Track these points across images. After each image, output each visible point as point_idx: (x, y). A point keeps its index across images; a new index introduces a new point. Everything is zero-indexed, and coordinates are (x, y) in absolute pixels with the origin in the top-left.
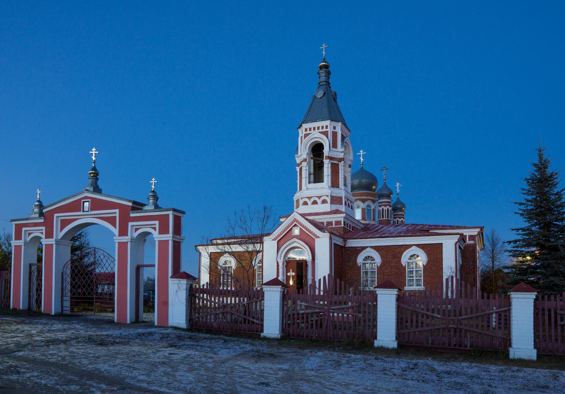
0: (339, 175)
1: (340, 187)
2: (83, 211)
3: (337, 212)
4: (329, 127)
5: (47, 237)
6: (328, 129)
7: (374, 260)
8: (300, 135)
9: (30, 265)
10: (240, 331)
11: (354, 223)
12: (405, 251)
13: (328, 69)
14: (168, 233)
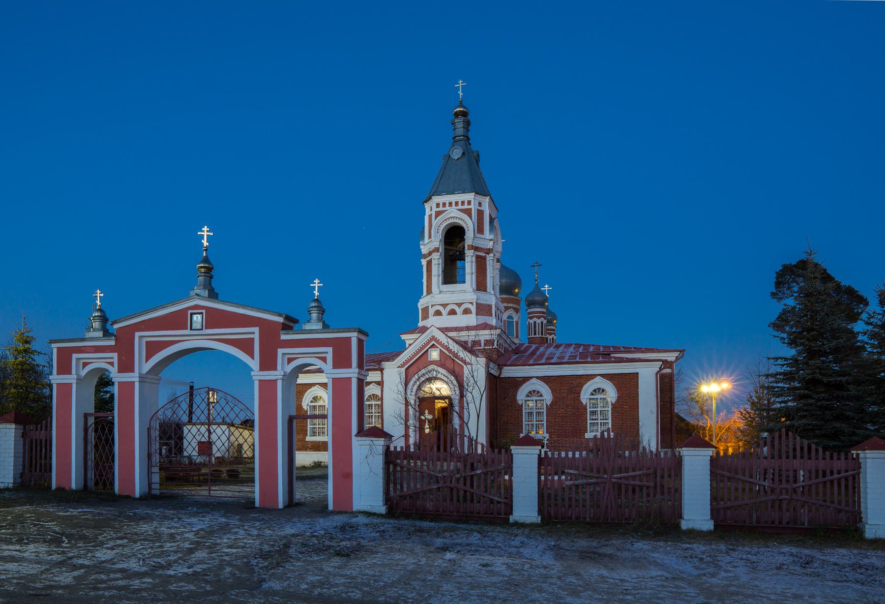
0: (486, 274)
1: (488, 290)
2: (191, 329)
3: (485, 326)
4: (472, 203)
5: (121, 370)
6: (472, 206)
7: (541, 396)
8: (428, 212)
9: (86, 416)
10: (472, 515)
11: (507, 342)
12: (586, 383)
13: (467, 117)
14: (350, 366)
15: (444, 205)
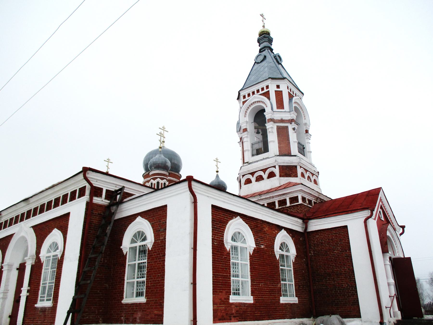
15: (249, 95)
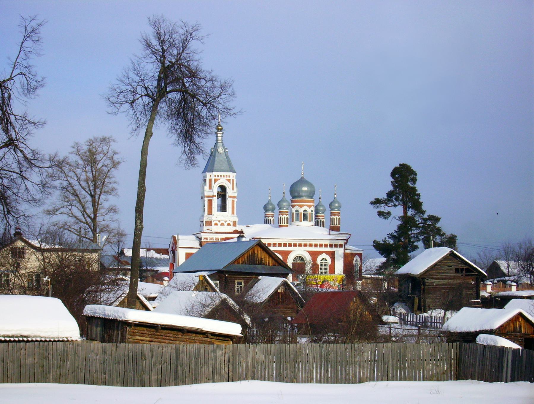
15: (218, 176)
